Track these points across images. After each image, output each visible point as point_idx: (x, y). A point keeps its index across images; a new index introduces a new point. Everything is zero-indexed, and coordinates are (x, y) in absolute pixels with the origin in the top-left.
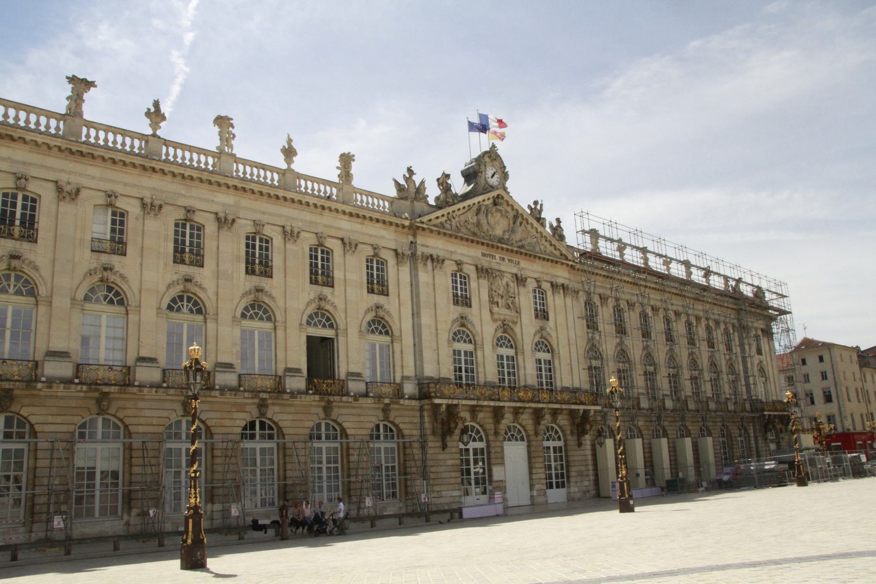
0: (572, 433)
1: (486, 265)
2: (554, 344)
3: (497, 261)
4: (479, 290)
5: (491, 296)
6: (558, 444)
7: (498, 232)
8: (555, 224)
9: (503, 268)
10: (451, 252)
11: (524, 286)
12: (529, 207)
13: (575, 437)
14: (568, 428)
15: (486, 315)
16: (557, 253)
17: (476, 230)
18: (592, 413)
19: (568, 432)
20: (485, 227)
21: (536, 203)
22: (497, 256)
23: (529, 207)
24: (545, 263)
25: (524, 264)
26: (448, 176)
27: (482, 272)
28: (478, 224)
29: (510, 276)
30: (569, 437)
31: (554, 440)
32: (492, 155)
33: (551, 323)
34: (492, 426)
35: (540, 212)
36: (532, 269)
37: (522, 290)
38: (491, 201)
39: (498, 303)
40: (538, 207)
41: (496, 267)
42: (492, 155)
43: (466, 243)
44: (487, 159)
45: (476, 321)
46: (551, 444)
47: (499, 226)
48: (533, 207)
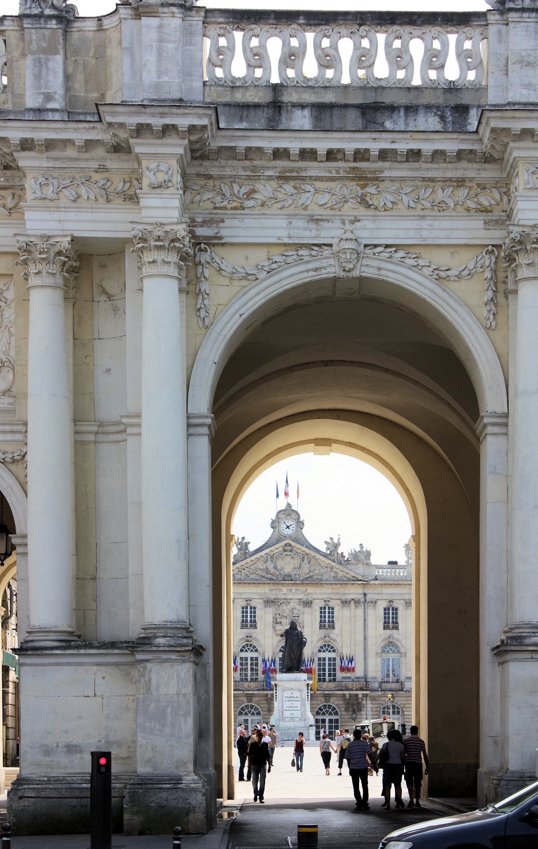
0: (347, 710)
1: (272, 597)
2: (337, 645)
3: (284, 592)
4: (265, 616)
5: (275, 619)
6: (334, 717)
7: (288, 570)
8: (358, 549)
9: (289, 597)
10: (241, 593)
11: (310, 607)
12: (326, 542)
13: (350, 713)
14: (343, 706)
15: (269, 631)
16: (349, 576)
17: (264, 574)
18: (360, 696)
19: (343, 709)
20: (273, 571)
21: (331, 539)
22: (284, 589)
23: (326, 542)
24: (334, 586)
25: (310, 590)
26: (243, 538)
27: (268, 602)
28: (267, 571)
29: (296, 601)
30: (344, 713)
31: (330, 714)
32: (289, 512)
33: (337, 631)
34: (266, 706)
35: (336, 546)
36: (319, 594)
37: (307, 610)
38: (281, 549)
39: (281, 622)
40: (336, 541)
41: (284, 597)
42: (289, 512)
43: (254, 585)
44: (282, 516)
45: (260, 637)
46: (327, 718)
47: (288, 565)
48: (330, 542)
